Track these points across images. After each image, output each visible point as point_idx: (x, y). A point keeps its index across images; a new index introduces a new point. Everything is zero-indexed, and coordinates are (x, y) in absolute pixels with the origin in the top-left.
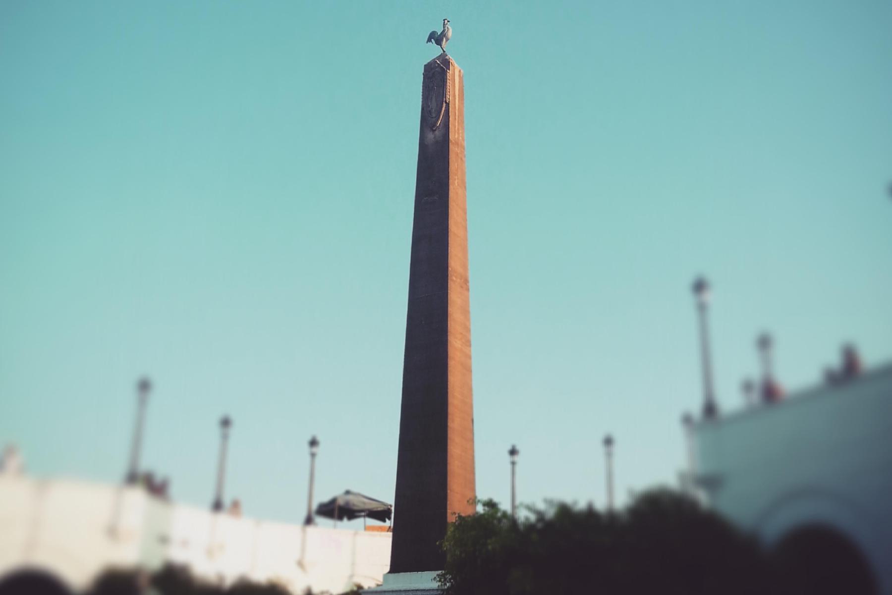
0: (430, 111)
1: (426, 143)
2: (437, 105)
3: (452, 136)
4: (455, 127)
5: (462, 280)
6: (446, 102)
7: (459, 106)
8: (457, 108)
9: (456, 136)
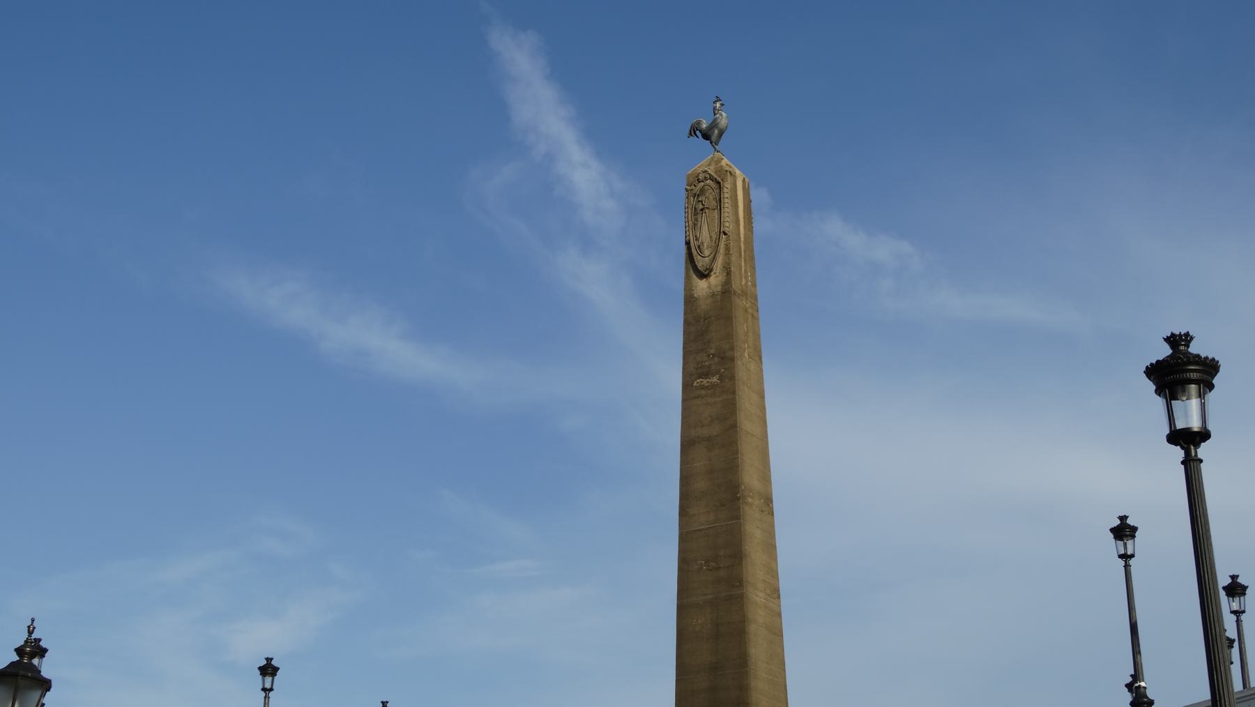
1: (696, 295)
2: (711, 237)
3: (736, 285)
4: (741, 269)
6: (725, 234)
8: (742, 239)
9: (743, 283)
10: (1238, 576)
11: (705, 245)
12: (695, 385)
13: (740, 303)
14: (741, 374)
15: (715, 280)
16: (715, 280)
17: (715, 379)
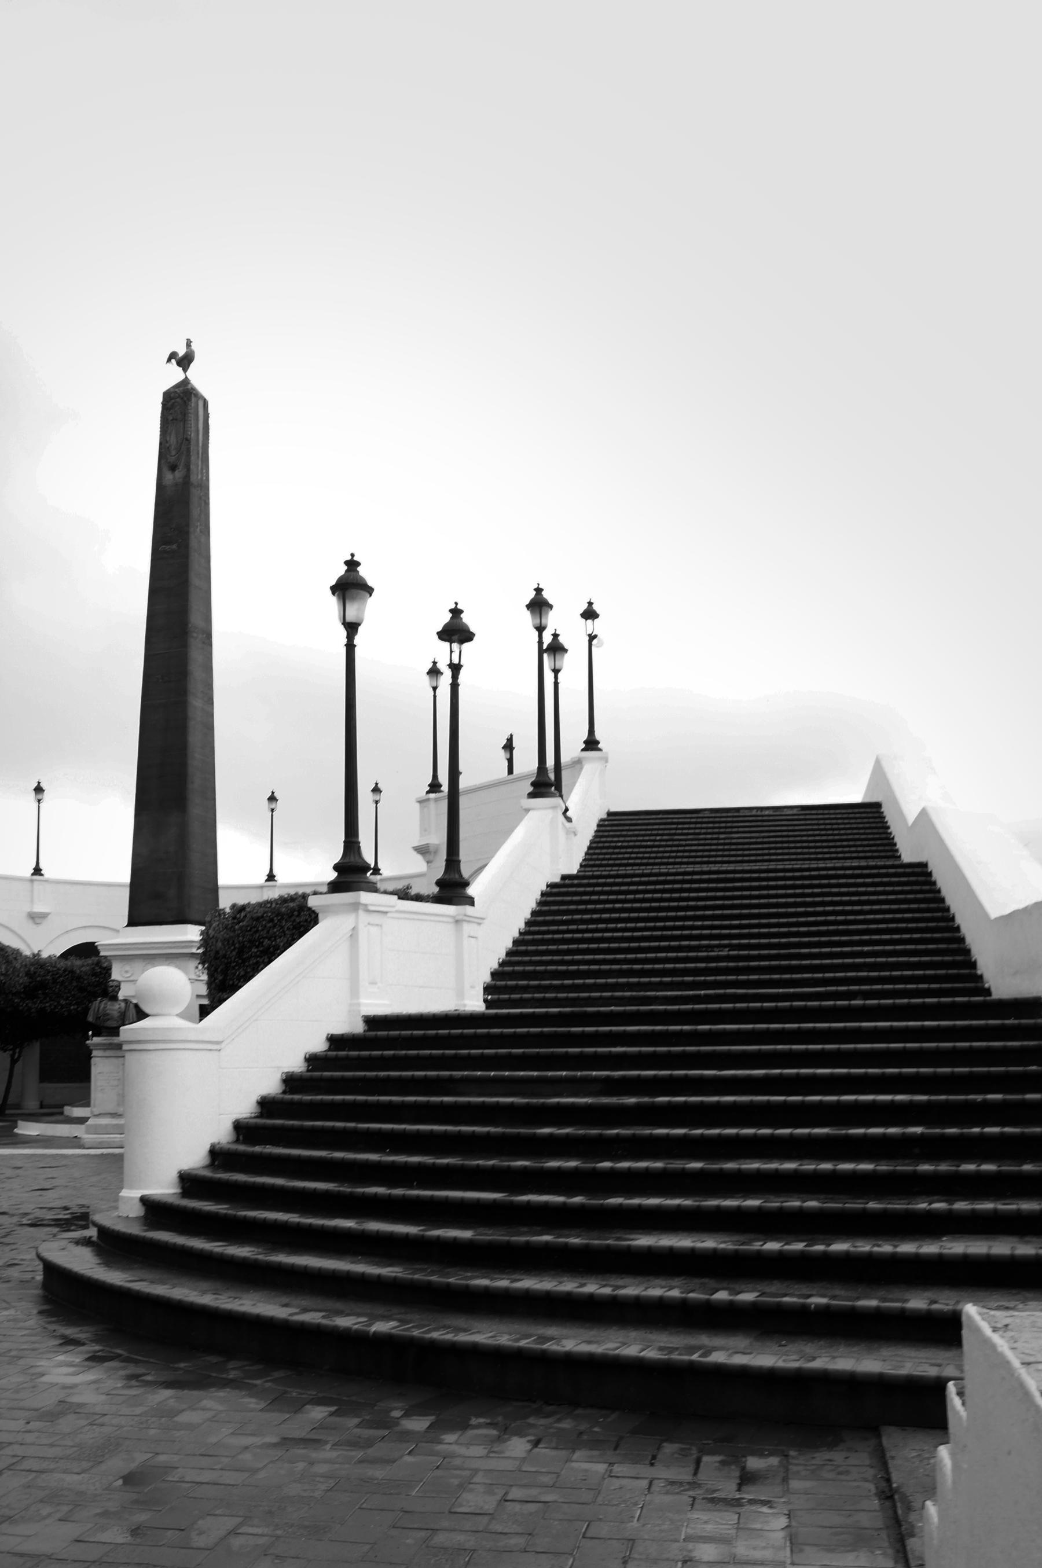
0: (168, 448)
1: (164, 484)
2: (177, 442)
3: (194, 479)
4: (198, 466)
5: (204, 636)
6: (187, 440)
7: (203, 441)
8: (200, 444)
9: (200, 477)
10: (413, 847)
11: (173, 447)
13: (195, 493)
14: (193, 543)
15: (179, 474)
16: (179, 474)
17: (174, 547)
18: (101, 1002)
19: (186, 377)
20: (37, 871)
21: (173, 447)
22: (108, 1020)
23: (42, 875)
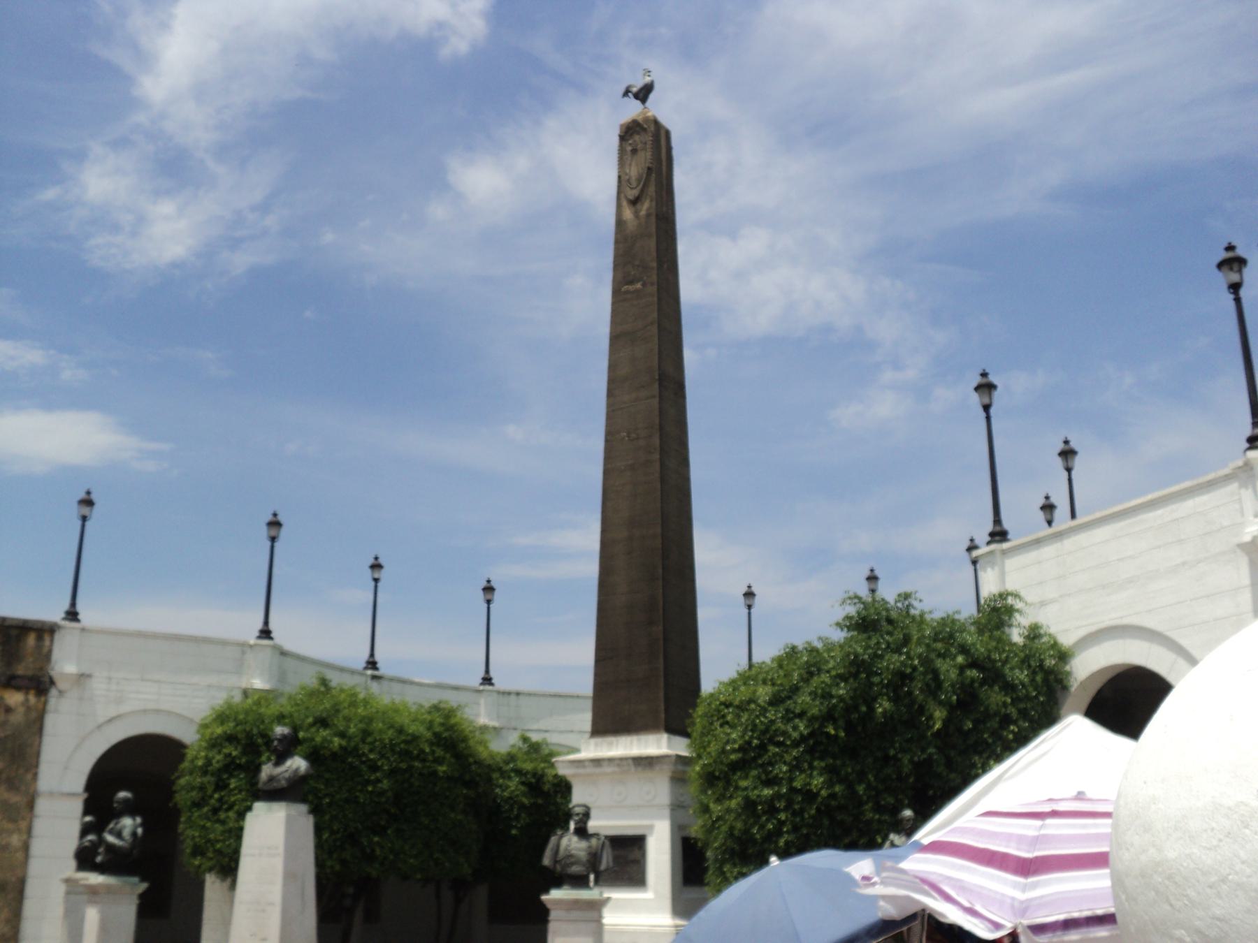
9: (664, 209)
12: (623, 289)
17: (639, 286)
18: (561, 837)
19: (645, 108)
20: (487, 680)
21: (634, 178)
22: (573, 864)
23: (492, 684)
